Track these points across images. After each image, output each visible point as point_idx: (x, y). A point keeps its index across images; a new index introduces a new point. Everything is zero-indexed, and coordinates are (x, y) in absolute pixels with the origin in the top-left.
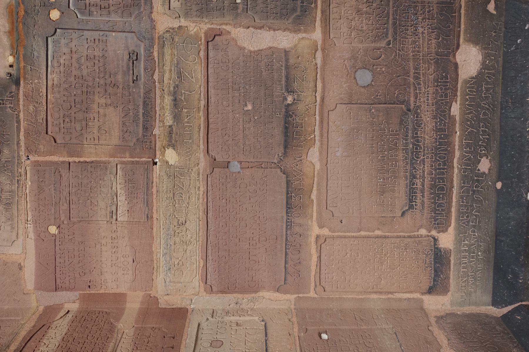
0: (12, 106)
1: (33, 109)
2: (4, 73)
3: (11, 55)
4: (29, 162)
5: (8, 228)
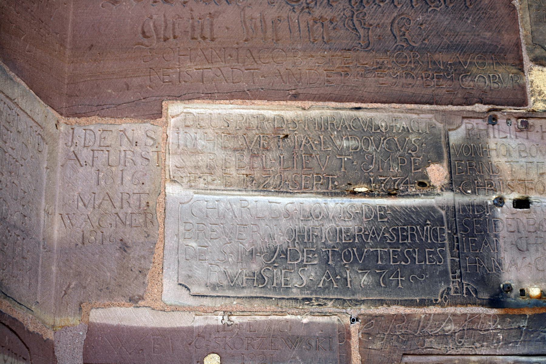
0: (452, 293)
1: (450, 330)
2: (510, 280)
3: (541, 291)
4: (347, 321)
5: (214, 279)
